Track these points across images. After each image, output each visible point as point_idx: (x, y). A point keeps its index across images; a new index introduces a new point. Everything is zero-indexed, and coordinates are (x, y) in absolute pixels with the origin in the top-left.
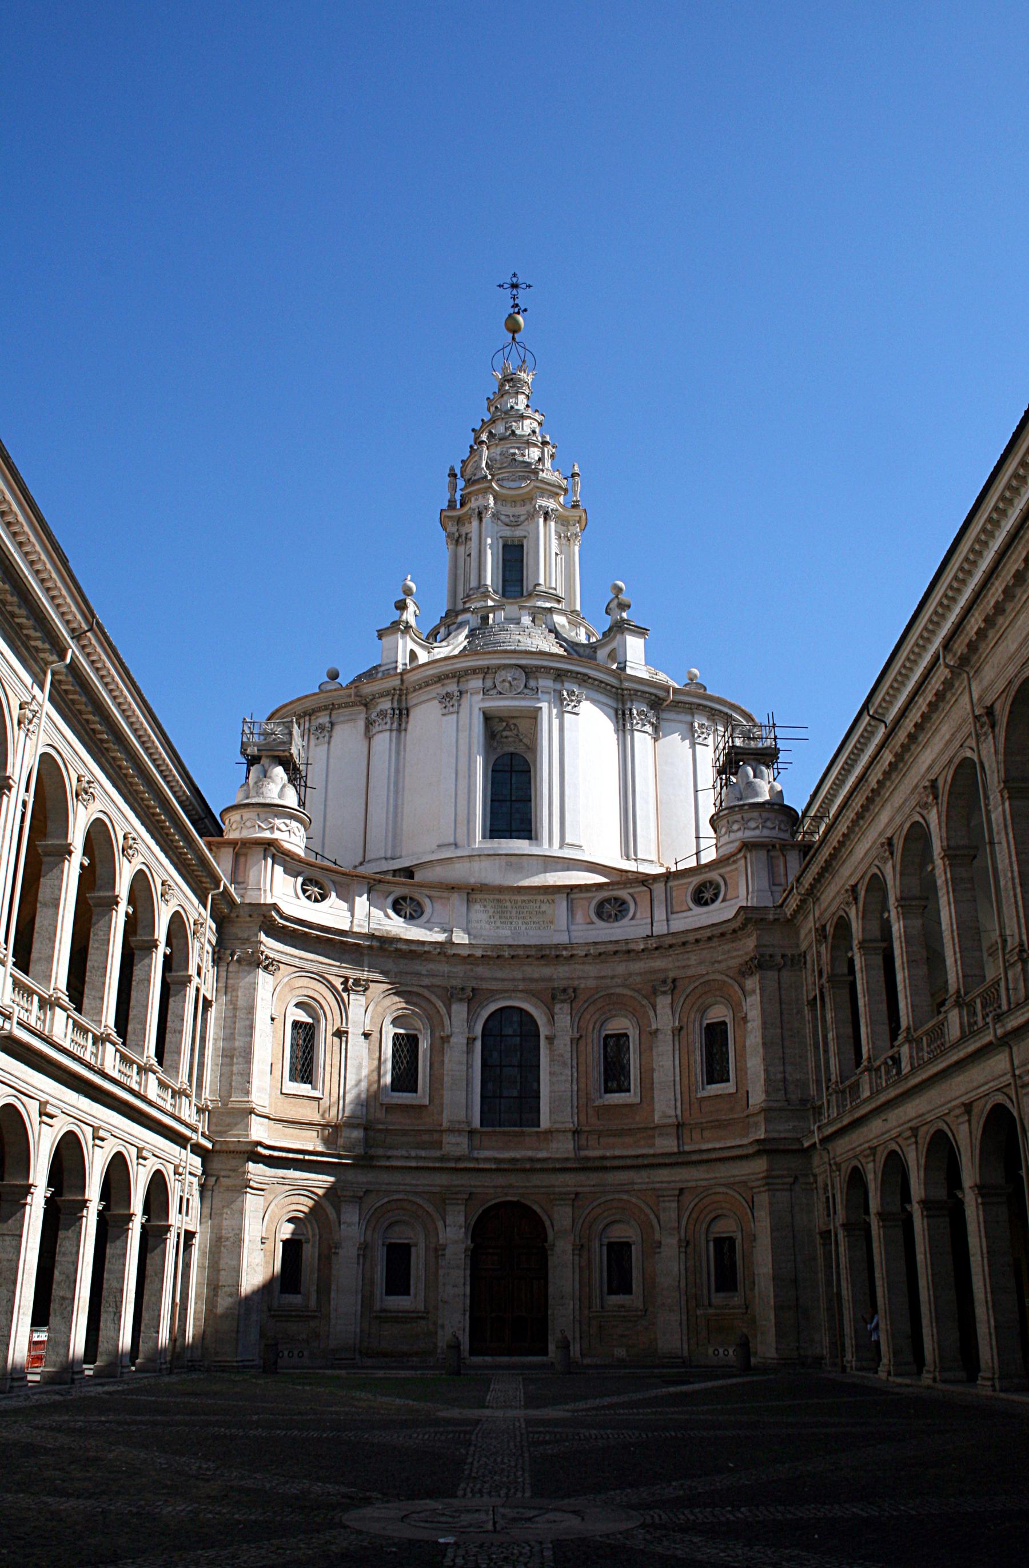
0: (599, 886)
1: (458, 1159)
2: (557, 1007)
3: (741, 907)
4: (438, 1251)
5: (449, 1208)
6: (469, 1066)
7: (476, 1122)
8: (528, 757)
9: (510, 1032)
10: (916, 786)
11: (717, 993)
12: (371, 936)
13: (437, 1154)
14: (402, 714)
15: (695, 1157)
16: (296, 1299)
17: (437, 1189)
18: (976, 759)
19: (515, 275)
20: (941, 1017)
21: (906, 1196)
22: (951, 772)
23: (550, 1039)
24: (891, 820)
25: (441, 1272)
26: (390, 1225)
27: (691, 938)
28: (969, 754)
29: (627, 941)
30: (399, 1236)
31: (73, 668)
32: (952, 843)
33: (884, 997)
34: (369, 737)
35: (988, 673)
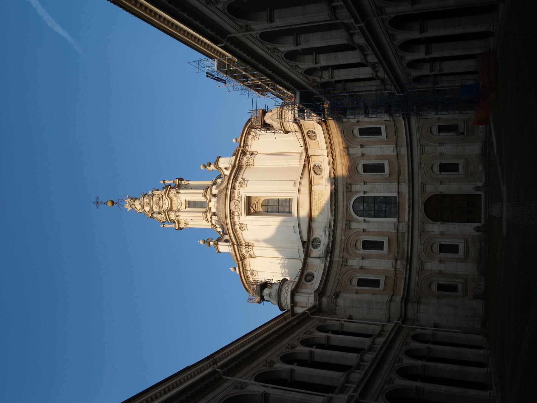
0: (310, 174)
1: (409, 227)
2: (353, 190)
3: (319, 123)
4: (442, 234)
5: (426, 230)
6: (374, 222)
7: (395, 220)
8: (263, 199)
9: (362, 207)
10: (271, 56)
11: (348, 131)
12: (326, 257)
13: (406, 234)
14: (248, 245)
15: (409, 140)
16: (460, 286)
17: (419, 234)
18: (260, 32)
19: (94, 203)
20: (356, 46)
21: (423, 61)
22: (265, 42)
23: (365, 192)
24: (284, 66)
25: (450, 233)
26: (432, 251)
27: (328, 141)
28: (258, 36)
29: (329, 164)
30: (436, 248)
31: (221, 367)
32: (292, 42)
33: (349, 69)
34: (256, 257)
35: (228, 28)
